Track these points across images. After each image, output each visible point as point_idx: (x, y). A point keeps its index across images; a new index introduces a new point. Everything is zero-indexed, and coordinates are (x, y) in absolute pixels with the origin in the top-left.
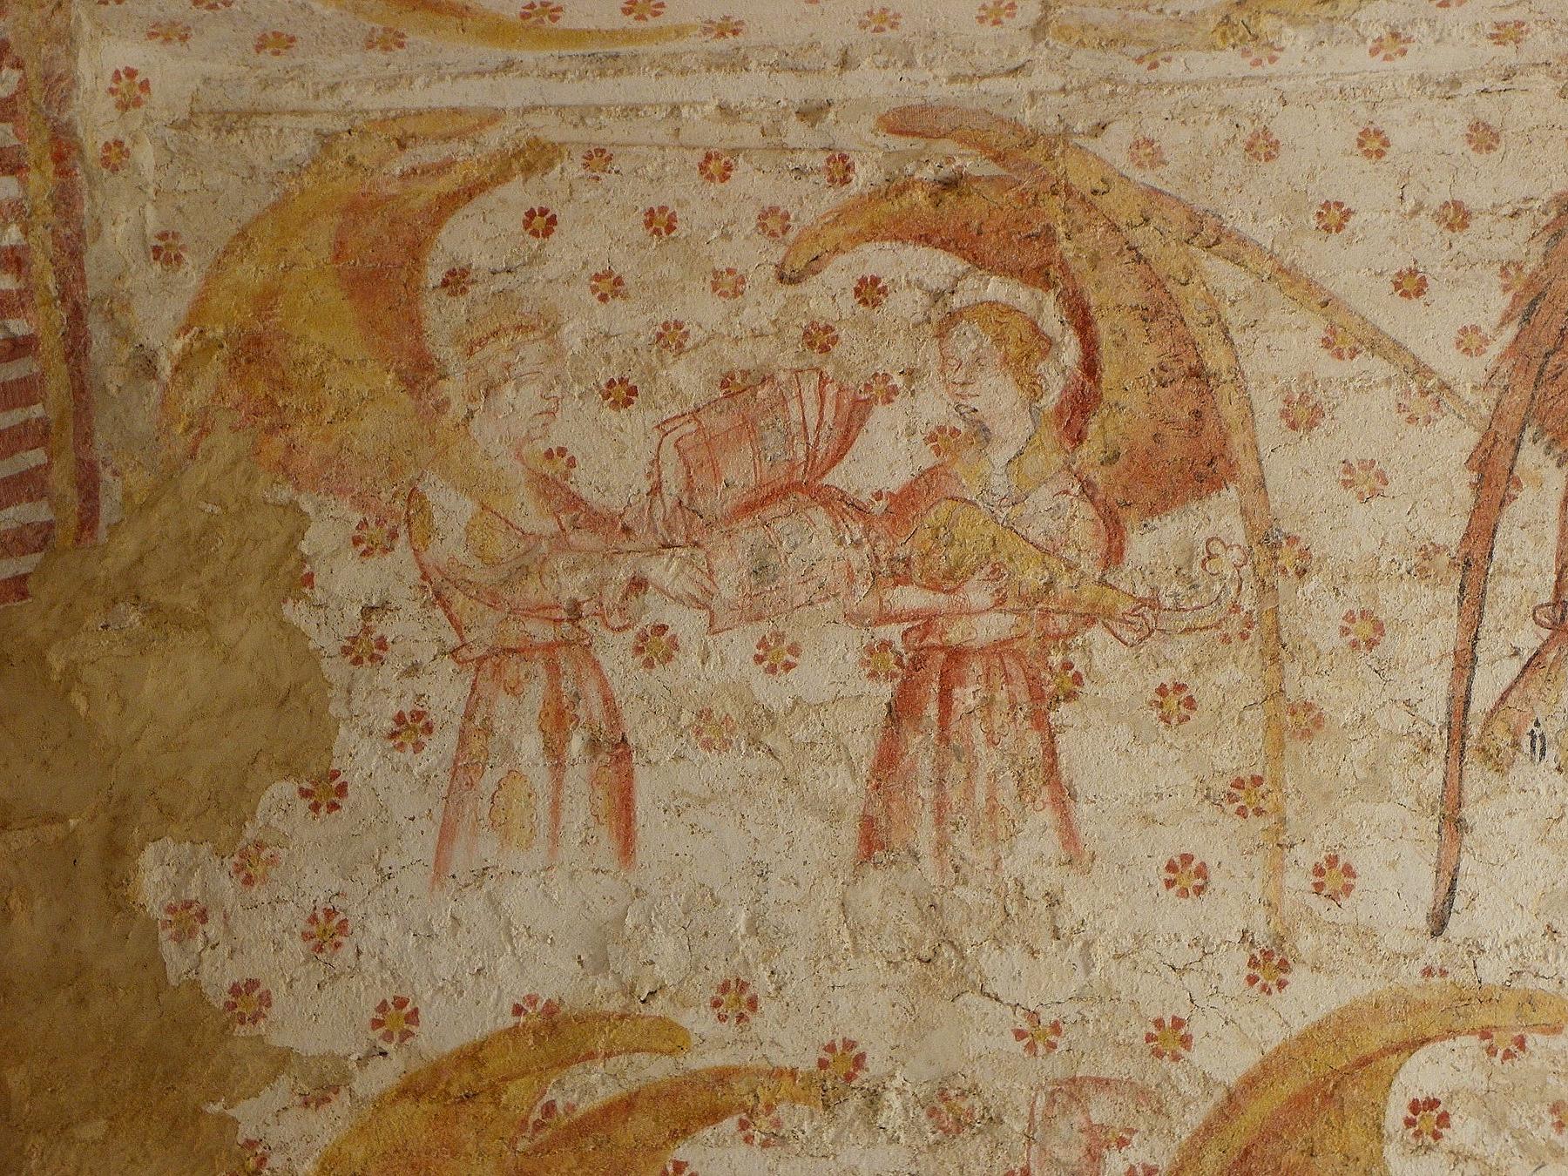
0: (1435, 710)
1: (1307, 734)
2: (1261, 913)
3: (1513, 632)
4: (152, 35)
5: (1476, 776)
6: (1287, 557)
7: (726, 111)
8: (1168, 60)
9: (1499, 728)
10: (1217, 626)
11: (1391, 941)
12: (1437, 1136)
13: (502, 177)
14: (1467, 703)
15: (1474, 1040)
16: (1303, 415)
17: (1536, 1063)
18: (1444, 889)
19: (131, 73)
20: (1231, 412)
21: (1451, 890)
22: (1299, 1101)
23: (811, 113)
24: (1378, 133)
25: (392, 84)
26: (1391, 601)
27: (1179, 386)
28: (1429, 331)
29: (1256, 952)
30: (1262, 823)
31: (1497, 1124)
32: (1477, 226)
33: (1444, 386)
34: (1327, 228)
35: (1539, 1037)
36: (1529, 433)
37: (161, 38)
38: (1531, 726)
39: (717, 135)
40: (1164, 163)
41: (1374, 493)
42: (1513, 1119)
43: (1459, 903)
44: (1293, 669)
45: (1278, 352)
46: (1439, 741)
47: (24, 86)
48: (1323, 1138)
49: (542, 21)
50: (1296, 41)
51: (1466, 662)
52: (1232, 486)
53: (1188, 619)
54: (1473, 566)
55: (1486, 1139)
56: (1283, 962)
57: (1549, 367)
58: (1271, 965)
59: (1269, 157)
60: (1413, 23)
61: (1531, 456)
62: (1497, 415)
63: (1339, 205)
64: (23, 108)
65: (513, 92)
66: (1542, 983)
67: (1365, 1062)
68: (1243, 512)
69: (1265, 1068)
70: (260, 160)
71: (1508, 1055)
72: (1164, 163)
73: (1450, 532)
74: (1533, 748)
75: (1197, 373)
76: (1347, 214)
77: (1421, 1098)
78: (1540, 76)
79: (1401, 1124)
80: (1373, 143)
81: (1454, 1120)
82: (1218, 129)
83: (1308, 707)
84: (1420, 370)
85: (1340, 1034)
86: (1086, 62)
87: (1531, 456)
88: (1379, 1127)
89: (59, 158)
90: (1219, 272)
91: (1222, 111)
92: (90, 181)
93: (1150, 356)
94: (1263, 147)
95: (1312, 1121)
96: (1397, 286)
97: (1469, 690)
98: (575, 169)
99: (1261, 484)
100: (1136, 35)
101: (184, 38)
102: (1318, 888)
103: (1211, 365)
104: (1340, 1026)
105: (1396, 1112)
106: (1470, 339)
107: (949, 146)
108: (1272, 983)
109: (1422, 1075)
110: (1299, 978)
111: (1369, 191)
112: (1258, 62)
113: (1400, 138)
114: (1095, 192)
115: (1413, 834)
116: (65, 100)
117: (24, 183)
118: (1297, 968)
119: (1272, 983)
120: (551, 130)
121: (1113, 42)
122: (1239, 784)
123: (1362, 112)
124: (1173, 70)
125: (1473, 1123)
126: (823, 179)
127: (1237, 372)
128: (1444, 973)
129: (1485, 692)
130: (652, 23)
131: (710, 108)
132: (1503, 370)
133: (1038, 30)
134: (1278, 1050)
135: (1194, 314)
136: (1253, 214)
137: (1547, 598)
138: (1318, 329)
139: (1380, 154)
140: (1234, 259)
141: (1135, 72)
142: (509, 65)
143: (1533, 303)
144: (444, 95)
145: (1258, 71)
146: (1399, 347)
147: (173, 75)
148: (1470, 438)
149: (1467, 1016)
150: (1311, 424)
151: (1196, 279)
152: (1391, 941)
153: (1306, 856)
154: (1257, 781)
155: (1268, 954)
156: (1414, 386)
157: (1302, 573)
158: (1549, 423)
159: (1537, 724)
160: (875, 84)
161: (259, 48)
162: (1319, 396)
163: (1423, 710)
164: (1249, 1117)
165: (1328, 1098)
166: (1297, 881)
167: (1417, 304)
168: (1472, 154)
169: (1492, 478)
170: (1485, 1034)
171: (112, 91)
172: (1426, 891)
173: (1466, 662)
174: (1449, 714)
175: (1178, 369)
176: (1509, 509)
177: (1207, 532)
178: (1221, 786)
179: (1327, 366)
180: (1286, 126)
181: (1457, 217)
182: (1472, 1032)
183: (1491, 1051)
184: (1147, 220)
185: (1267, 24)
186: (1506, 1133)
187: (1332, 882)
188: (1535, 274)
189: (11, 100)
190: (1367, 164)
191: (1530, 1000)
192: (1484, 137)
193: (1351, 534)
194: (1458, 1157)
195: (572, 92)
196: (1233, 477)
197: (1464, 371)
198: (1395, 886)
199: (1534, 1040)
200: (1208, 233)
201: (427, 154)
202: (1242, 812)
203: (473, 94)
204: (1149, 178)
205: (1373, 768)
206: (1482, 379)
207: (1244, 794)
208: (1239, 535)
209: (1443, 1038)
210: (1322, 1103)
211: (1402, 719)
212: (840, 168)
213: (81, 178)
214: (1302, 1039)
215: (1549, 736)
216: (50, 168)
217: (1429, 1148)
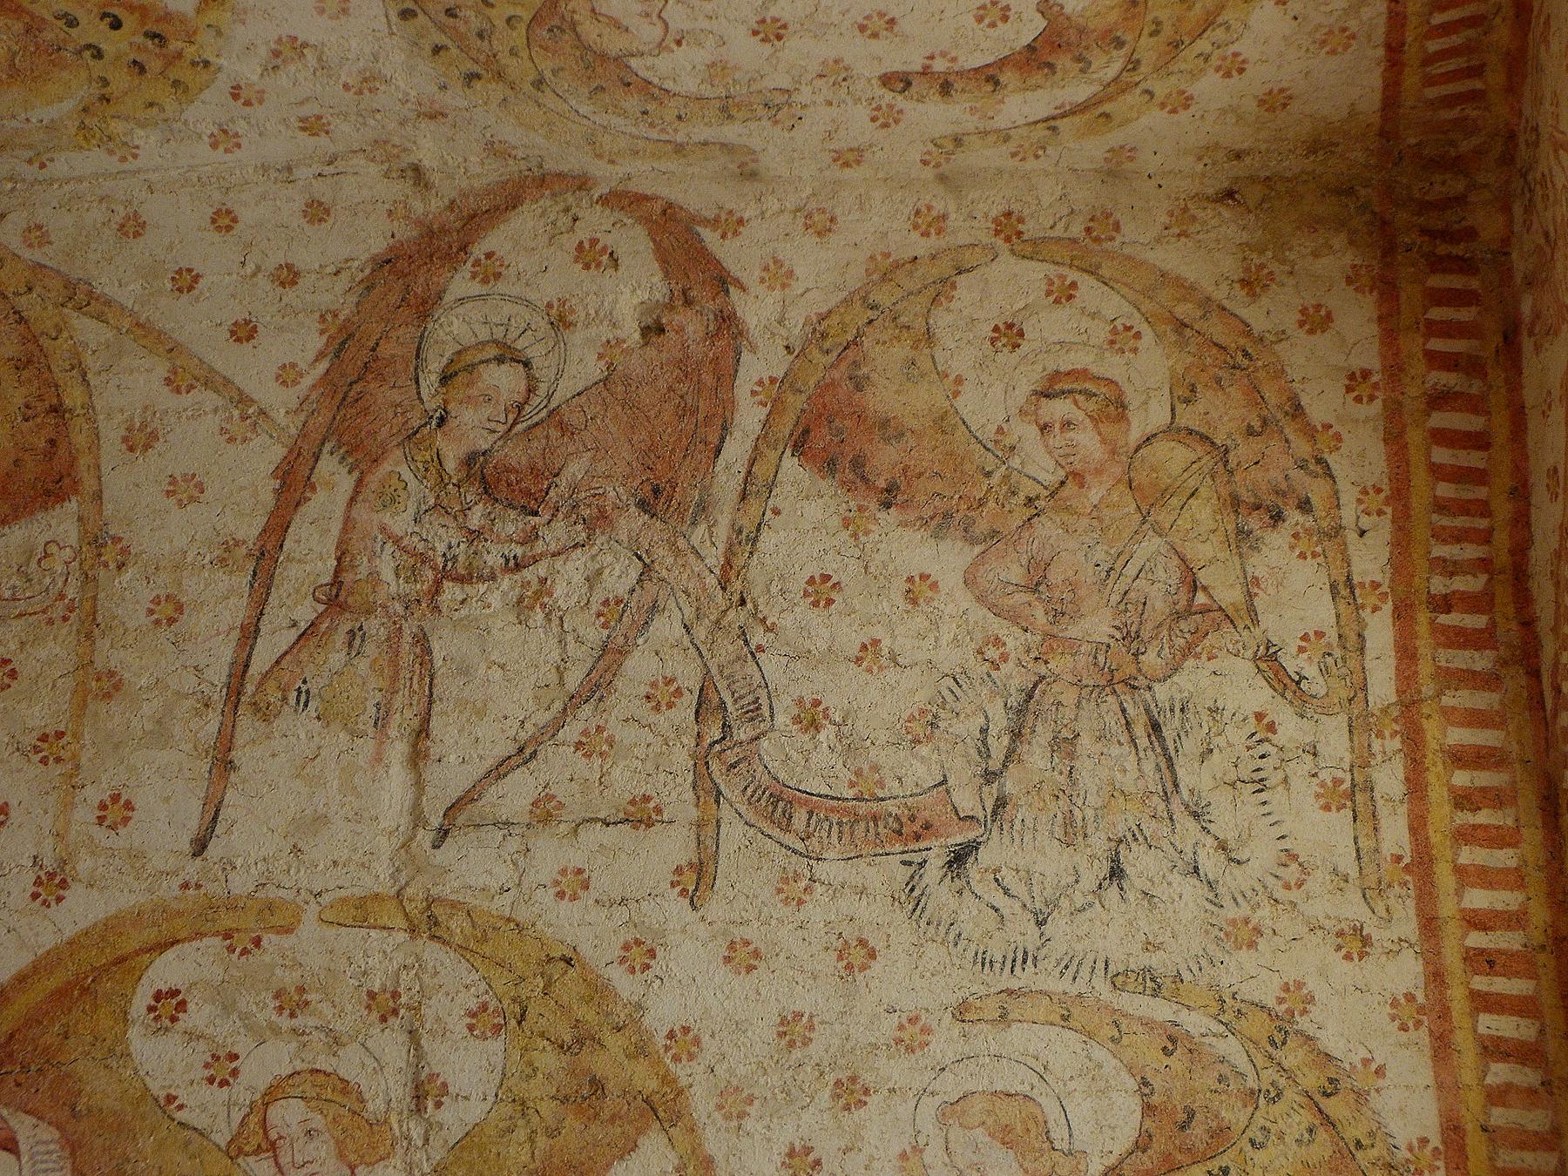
0: (218, 674)
1: (108, 696)
2: (49, 842)
3: (293, 605)
5: (247, 725)
6: (110, 555)
8: (52, 160)
9: (271, 685)
10: (44, 612)
11: (157, 862)
12: (174, 1019)
14: (247, 666)
15: (217, 941)
16: (140, 439)
17: (267, 959)
18: (208, 817)
20: (80, 439)
21: (215, 819)
22: (61, 994)
24: (229, 212)
26: (192, 587)
27: (39, 420)
28: (253, 370)
29: (42, 873)
30: (59, 769)
31: (228, 1009)
32: (305, 282)
33: (262, 412)
34: (180, 290)
35: (273, 937)
36: (328, 447)
38: (299, 683)
40: (50, 243)
41: (192, 499)
42: (242, 1005)
43: (219, 830)
44: (103, 644)
45: (126, 388)
46: (218, 697)
48: (77, 1023)
50: (147, 140)
51: (250, 634)
52: (74, 499)
53: (22, 606)
54: (266, 557)
55: (218, 1021)
56: (64, 881)
57: (351, 394)
58: (52, 884)
59: (137, 234)
60: (232, 120)
61: (328, 465)
62: (303, 434)
63: (189, 270)
66: (281, 893)
67: (120, 961)
68: (80, 519)
69: (35, 968)
71: (245, 952)
72: (50, 243)
73: (250, 530)
74: (298, 701)
75: (56, 410)
76: (196, 278)
77: (165, 989)
78: (360, 160)
79: (144, 1011)
80: (224, 220)
81: (191, 1007)
82: (97, 214)
83: (111, 674)
84: (243, 400)
85: (103, 938)
87: (328, 465)
88: (126, 1013)
90: (87, 330)
91: (101, 200)
93: (18, 398)
94: (133, 227)
95: (70, 1010)
96: (233, 333)
97: (249, 656)
99: (98, 496)
102: (101, 820)
103: (68, 402)
104: (110, 927)
105: (141, 1001)
106: (287, 375)
108: (51, 899)
109: (166, 971)
110: (76, 896)
111: (216, 260)
112: (123, 159)
113: (247, 215)
115: (188, 775)
118: (74, 886)
119: (51, 899)
122: (44, 738)
123: (217, 196)
125: (207, 1008)
127: (89, 406)
128: (198, 886)
129: (262, 658)
132: (314, 396)
134: (48, 953)
135: (59, 364)
136: (118, 281)
137: (327, 579)
138: (162, 370)
139: (229, 228)
140: (100, 317)
141: (30, 172)
143: (344, 343)
146: (227, 382)
148: (278, 452)
149: (214, 920)
150: (147, 447)
151: (65, 335)
152: (157, 862)
153: (94, 795)
154: (60, 735)
155: (51, 876)
156: (236, 413)
157: (121, 566)
158: (345, 438)
159: (305, 682)
162: (156, 424)
163: (209, 674)
164: (16, 1007)
165: (85, 990)
166: (84, 815)
167: (247, 347)
168: (306, 226)
169: (293, 484)
170: (228, 936)
172: (192, 818)
173: (250, 634)
174: (230, 676)
175: (41, 407)
176: (302, 509)
177: (47, 536)
178: (30, 740)
179: (167, 400)
181: (288, 276)
182: (217, 934)
183: (231, 949)
184: (30, 289)
185: (117, 127)
186: (235, 1017)
187: (113, 815)
188: (347, 320)
190: (216, 237)
191: (270, 907)
192: (317, 212)
193: (161, 531)
194: (191, 1036)
196: (76, 492)
197: (279, 401)
198: (164, 819)
199: (269, 939)
200: (79, 296)
202: (44, 761)
204: (35, 255)
205: (159, 722)
206: (294, 404)
207: (48, 746)
208: (73, 538)
209: (190, 939)
210: (81, 995)
211: (190, 682)
214: (70, 943)
215: (314, 691)
217: (167, 1029)
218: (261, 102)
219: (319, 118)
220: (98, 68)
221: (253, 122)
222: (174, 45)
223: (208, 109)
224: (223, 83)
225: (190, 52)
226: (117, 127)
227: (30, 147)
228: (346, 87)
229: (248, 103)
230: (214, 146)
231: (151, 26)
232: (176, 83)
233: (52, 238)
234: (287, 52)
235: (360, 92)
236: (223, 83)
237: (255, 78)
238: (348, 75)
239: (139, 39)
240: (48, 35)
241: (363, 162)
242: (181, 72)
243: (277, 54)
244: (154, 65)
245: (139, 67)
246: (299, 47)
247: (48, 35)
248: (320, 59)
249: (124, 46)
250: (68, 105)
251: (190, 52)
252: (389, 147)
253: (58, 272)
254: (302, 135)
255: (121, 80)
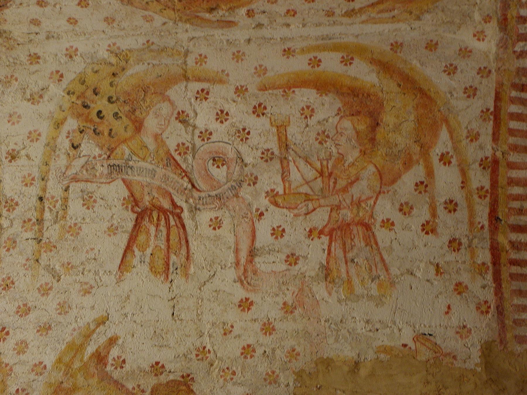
4: (470, 51)
7: (288, 25)
13: (361, 9)
19: (479, 39)
23: (260, 26)
24: (71, 23)
25: (396, 30)
37: (468, 50)
39: (290, 20)
40: (142, 16)
47: (514, 45)
49: (347, 56)
50: (103, 54)
60: (66, 63)
64: (515, 37)
65: (356, 29)
70: (440, 14)
72: (142, 16)
78: (21, 40)
80: (72, 21)
86: (170, 42)
89: (506, 19)
91: (124, 29)
92: (496, 12)
94: (109, 20)
98: (338, 11)
100: (155, 54)
101: (460, 50)
107: (214, 19)
112: (114, 44)
114: (165, 9)
116: (501, 39)
117: (518, 13)
120: (345, 20)
121: (162, 50)
124: (142, 40)
126: (255, 11)
130: (311, 55)
131: (292, 27)
133: (187, 53)
142: (357, 36)
144: (379, 27)
145: (114, 41)
147: (466, 37)
160: (239, 35)
161: (437, 44)
168: (38, 18)
171: (486, 36)
180: (103, 26)
185: (113, 60)
189: (518, 41)
192: (35, 22)
195: (337, 30)
201: (386, 15)
203: (370, 28)
204: (146, 13)
212: (250, 14)
213: (499, 13)
216: (509, 16)
218: (52, 73)
219: (31, 63)
220: (112, 92)
221: (57, 62)
222: (79, 102)
223: (73, 70)
224: (65, 82)
225: (74, 99)
226: (113, 60)
227: (152, 51)
228: (16, 80)
229: (58, 72)
230: (77, 50)
231: (86, 111)
232: (83, 83)
233: (142, 18)
234: (36, 97)
235: (12, 76)
236: (65, 82)
237: (52, 85)
238: (15, 84)
239: (92, 105)
240: (127, 108)
241: (19, 39)
242: (80, 88)
243: (41, 96)
244: (89, 93)
245: (96, 92)
246: (32, 100)
247: (127, 108)
248: (24, 93)
249: (99, 103)
250: (129, 72)
251: (74, 99)
252: (7, 46)
253: (136, 8)
254: (40, 54)
255: (105, 87)
